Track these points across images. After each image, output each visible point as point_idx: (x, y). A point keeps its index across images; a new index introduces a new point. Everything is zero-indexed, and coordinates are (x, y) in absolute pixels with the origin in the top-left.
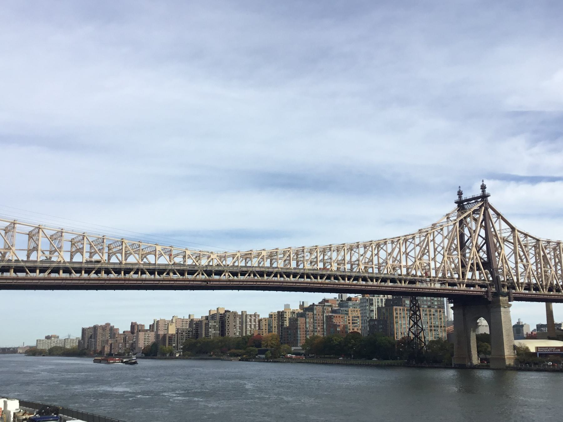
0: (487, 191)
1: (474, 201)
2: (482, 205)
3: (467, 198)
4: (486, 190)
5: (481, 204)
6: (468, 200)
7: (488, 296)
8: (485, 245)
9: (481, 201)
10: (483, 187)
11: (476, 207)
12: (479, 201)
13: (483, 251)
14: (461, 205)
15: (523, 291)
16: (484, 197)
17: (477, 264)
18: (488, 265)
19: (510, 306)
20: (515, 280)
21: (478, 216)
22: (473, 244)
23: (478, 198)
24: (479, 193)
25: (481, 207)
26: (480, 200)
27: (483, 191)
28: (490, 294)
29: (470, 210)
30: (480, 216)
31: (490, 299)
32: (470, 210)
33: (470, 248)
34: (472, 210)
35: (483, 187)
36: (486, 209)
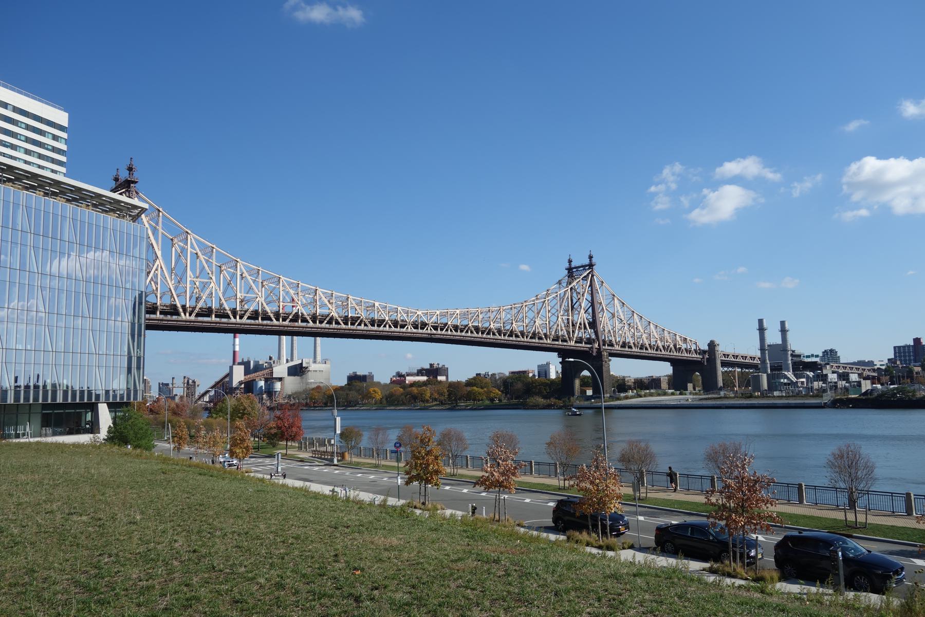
0: (594, 260)
1: (582, 269)
2: (589, 273)
5: (588, 272)
6: (575, 268)
8: (591, 308)
9: (588, 269)
10: (591, 257)
11: (585, 274)
13: (589, 314)
14: (571, 272)
15: (619, 349)
16: (591, 266)
17: (584, 324)
18: (593, 324)
19: (610, 360)
20: (614, 340)
21: (586, 282)
22: (581, 307)
23: (586, 266)
24: (587, 262)
25: (588, 274)
26: (587, 268)
27: (590, 260)
28: (595, 351)
30: (587, 282)
31: (594, 354)
32: (580, 278)
33: (579, 310)
34: (581, 277)
35: (591, 257)
36: (593, 276)
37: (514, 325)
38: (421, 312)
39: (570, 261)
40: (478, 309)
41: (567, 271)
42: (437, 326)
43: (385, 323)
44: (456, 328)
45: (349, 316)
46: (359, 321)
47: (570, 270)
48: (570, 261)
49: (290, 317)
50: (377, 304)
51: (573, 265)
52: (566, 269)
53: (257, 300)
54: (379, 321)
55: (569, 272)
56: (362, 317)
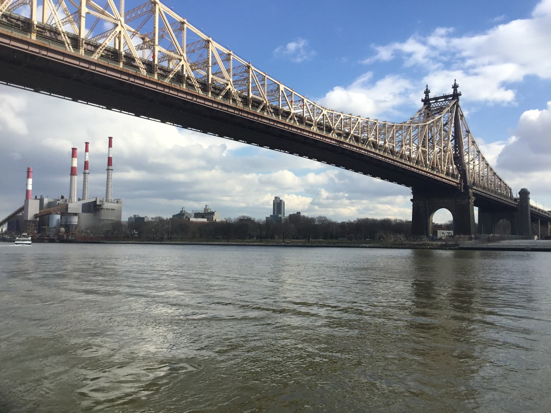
0: (459, 90)
1: (443, 99)
2: (455, 103)
3: (437, 96)
4: (457, 89)
6: (436, 99)
7: (461, 188)
10: (455, 87)
12: (450, 100)
16: (456, 96)
18: (458, 159)
23: (450, 96)
24: (451, 91)
25: (453, 105)
29: (449, 106)
35: (455, 87)
37: (404, 148)
38: (326, 111)
39: (427, 92)
40: (376, 121)
41: (423, 103)
42: (340, 134)
43: (290, 117)
44: (357, 139)
45: (250, 97)
46: (261, 107)
47: (426, 101)
48: (427, 92)
49: (171, 76)
50: (282, 87)
51: (431, 95)
52: (422, 101)
53: (118, 29)
54: (284, 112)
55: (424, 104)
56: (265, 102)
